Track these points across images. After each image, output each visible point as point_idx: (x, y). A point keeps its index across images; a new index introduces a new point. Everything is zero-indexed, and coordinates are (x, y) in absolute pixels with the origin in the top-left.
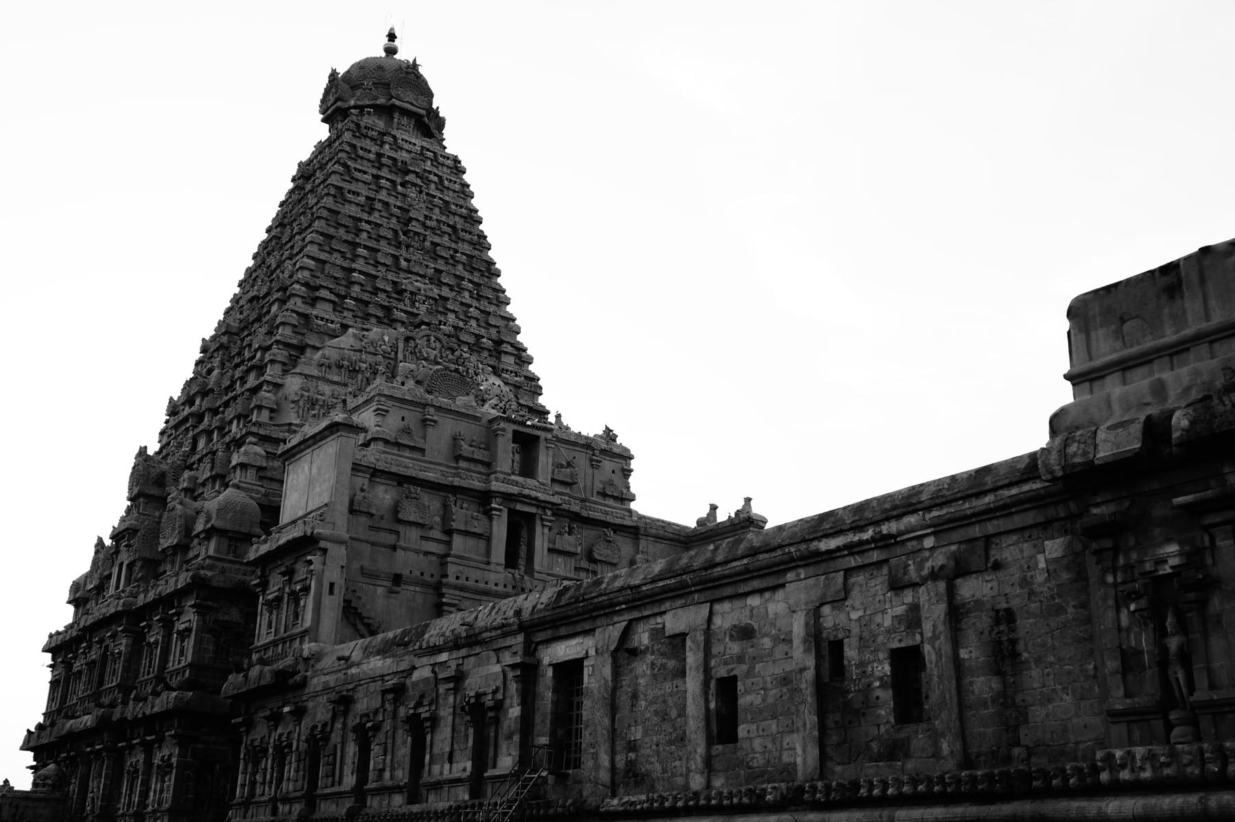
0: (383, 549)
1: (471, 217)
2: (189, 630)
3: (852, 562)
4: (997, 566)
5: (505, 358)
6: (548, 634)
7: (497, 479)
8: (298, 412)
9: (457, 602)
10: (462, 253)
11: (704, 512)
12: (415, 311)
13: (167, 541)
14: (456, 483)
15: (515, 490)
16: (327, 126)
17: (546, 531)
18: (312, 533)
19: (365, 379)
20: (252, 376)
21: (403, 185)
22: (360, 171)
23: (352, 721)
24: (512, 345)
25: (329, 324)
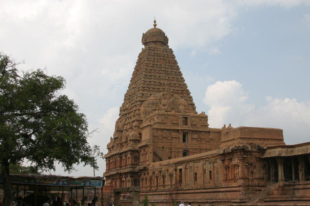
1: (175, 62)
2: (129, 158)
3: (206, 160)
4: (217, 162)
5: (184, 94)
6: (178, 165)
11: (223, 126)
13: (124, 140)
14: (172, 129)
15: (183, 128)
16: (144, 45)
17: (190, 135)
20: (135, 107)
21: (160, 59)
23: (155, 176)
24: (186, 91)
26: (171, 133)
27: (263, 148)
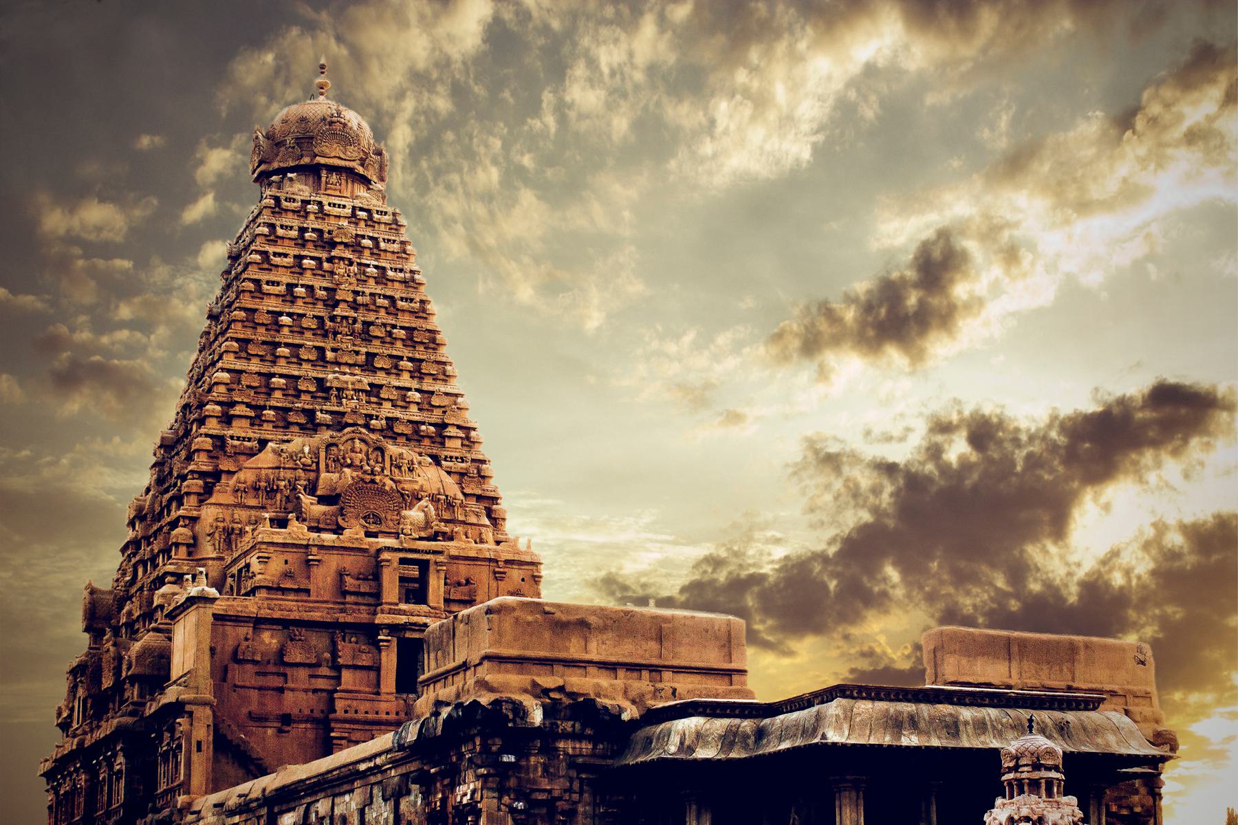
0: (271, 692)
1: (413, 280)
2: (120, 771)
3: (373, 779)
5: (448, 443)
7: (382, 612)
8: (214, 545)
9: (347, 735)
10: (402, 328)
12: (341, 409)
13: (107, 682)
15: (403, 619)
18: (178, 699)
19: (284, 499)
20: (174, 505)
21: (330, 260)
22: (280, 255)
24: (459, 427)
25: (246, 443)
26: (334, 643)
27: (620, 715)
